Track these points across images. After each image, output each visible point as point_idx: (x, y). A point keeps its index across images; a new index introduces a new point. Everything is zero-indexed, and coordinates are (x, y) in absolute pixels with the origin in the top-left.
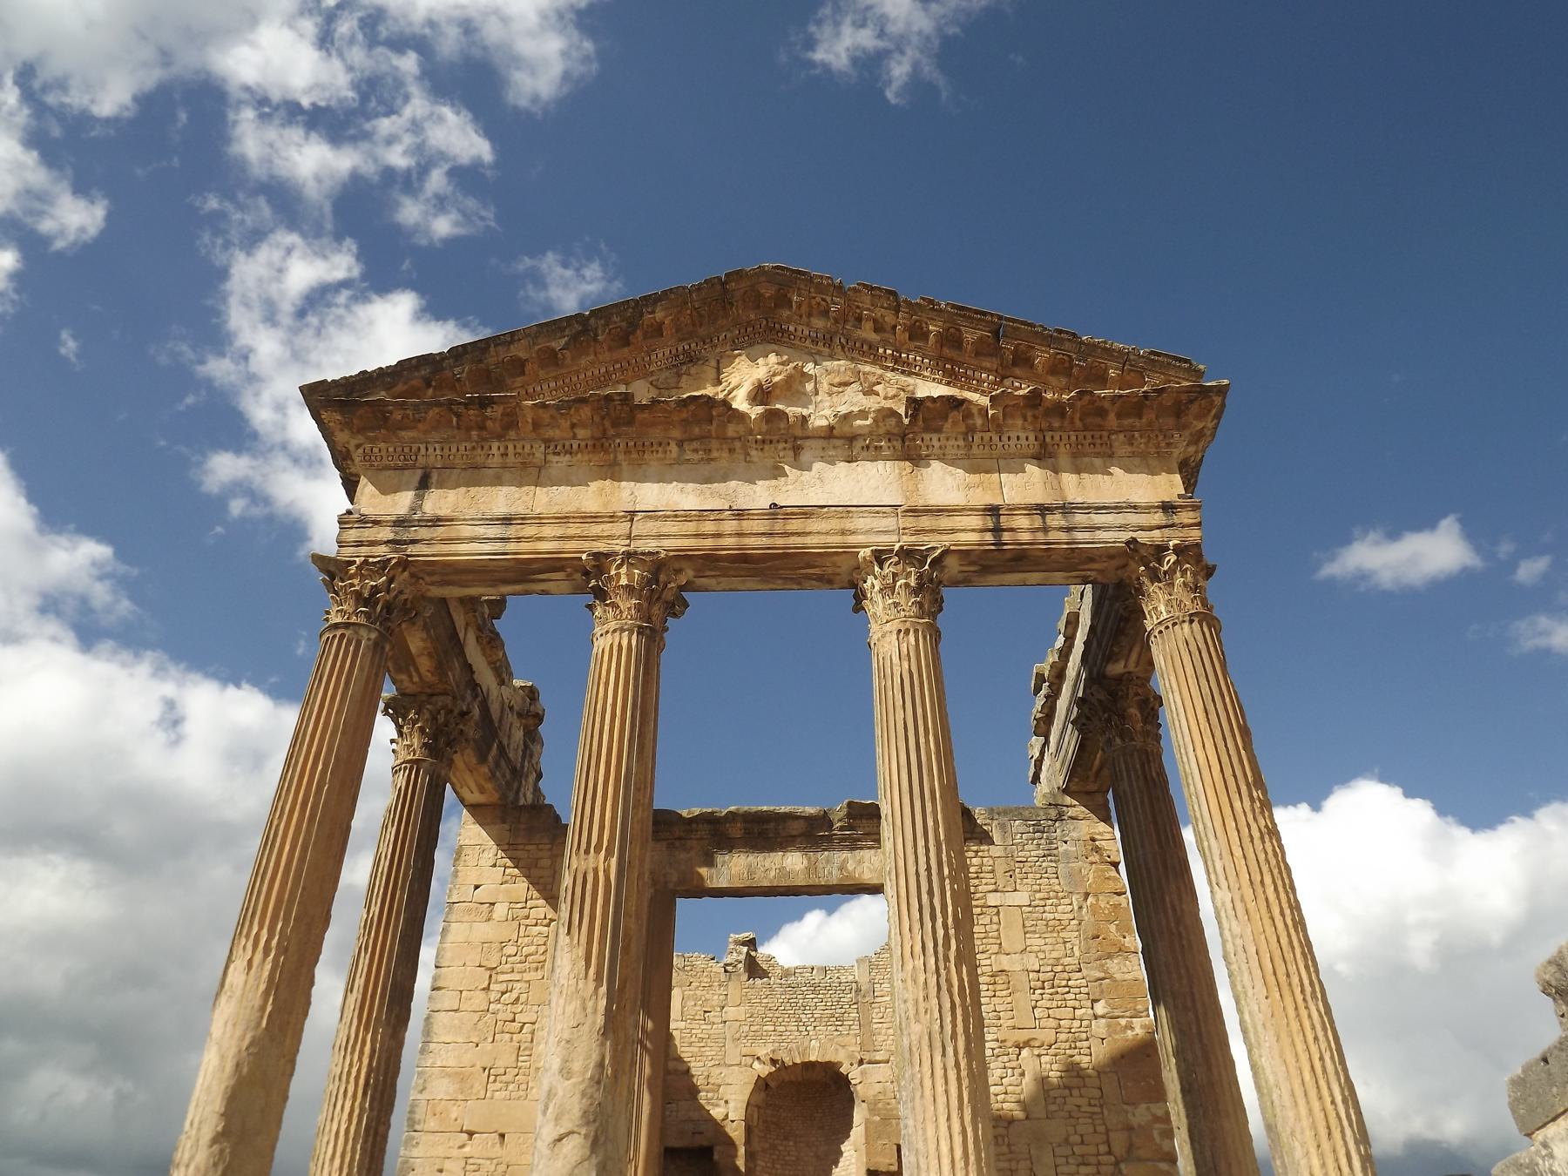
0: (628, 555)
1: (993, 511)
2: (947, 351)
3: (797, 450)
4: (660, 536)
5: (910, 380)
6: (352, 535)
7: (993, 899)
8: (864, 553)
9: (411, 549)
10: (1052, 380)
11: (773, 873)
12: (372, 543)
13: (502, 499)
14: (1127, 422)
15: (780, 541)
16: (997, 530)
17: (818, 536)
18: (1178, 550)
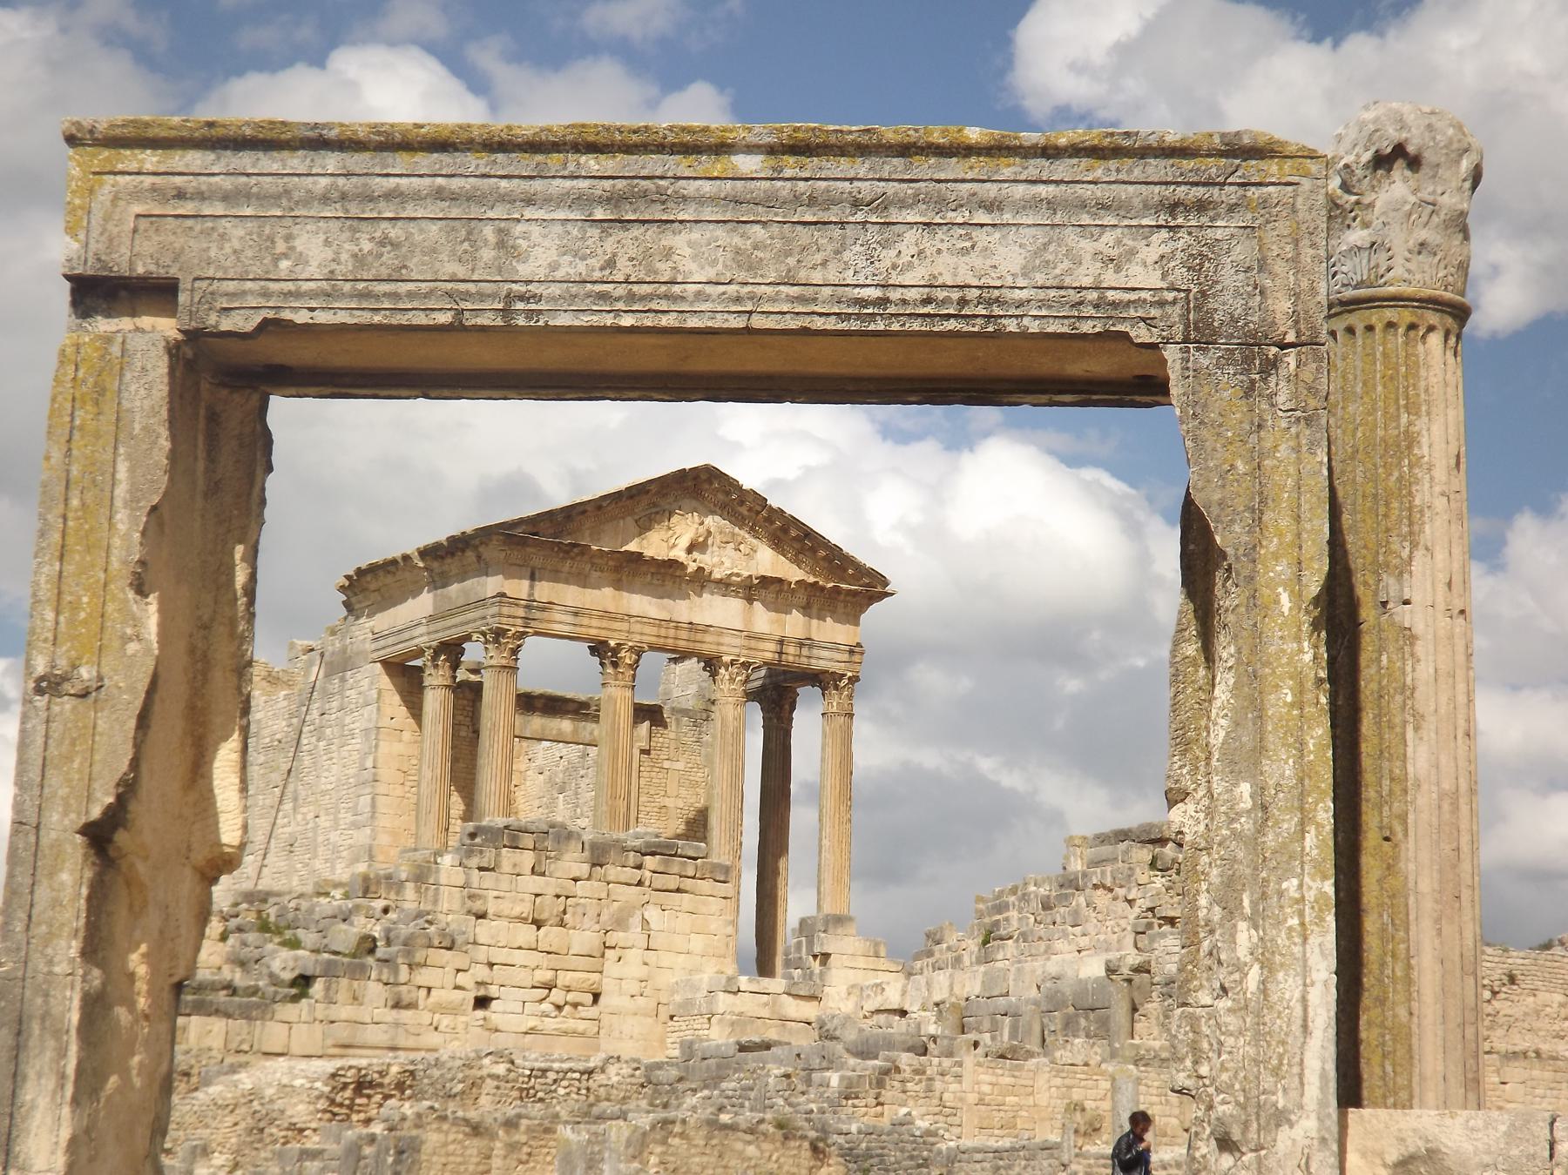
0: (632, 647)
1: (781, 642)
2: (778, 533)
3: (703, 587)
4: (642, 634)
5: (755, 541)
6: (505, 610)
7: (666, 764)
8: (727, 659)
9: (533, 624)
10: (821, 563)
11: (554, 732)
12: (514, 617)
13: (571, 595)
14: (849, 598)
15: (691, 645)
16: (781, 653)
17: (708, 646)
18: (850, 678)
